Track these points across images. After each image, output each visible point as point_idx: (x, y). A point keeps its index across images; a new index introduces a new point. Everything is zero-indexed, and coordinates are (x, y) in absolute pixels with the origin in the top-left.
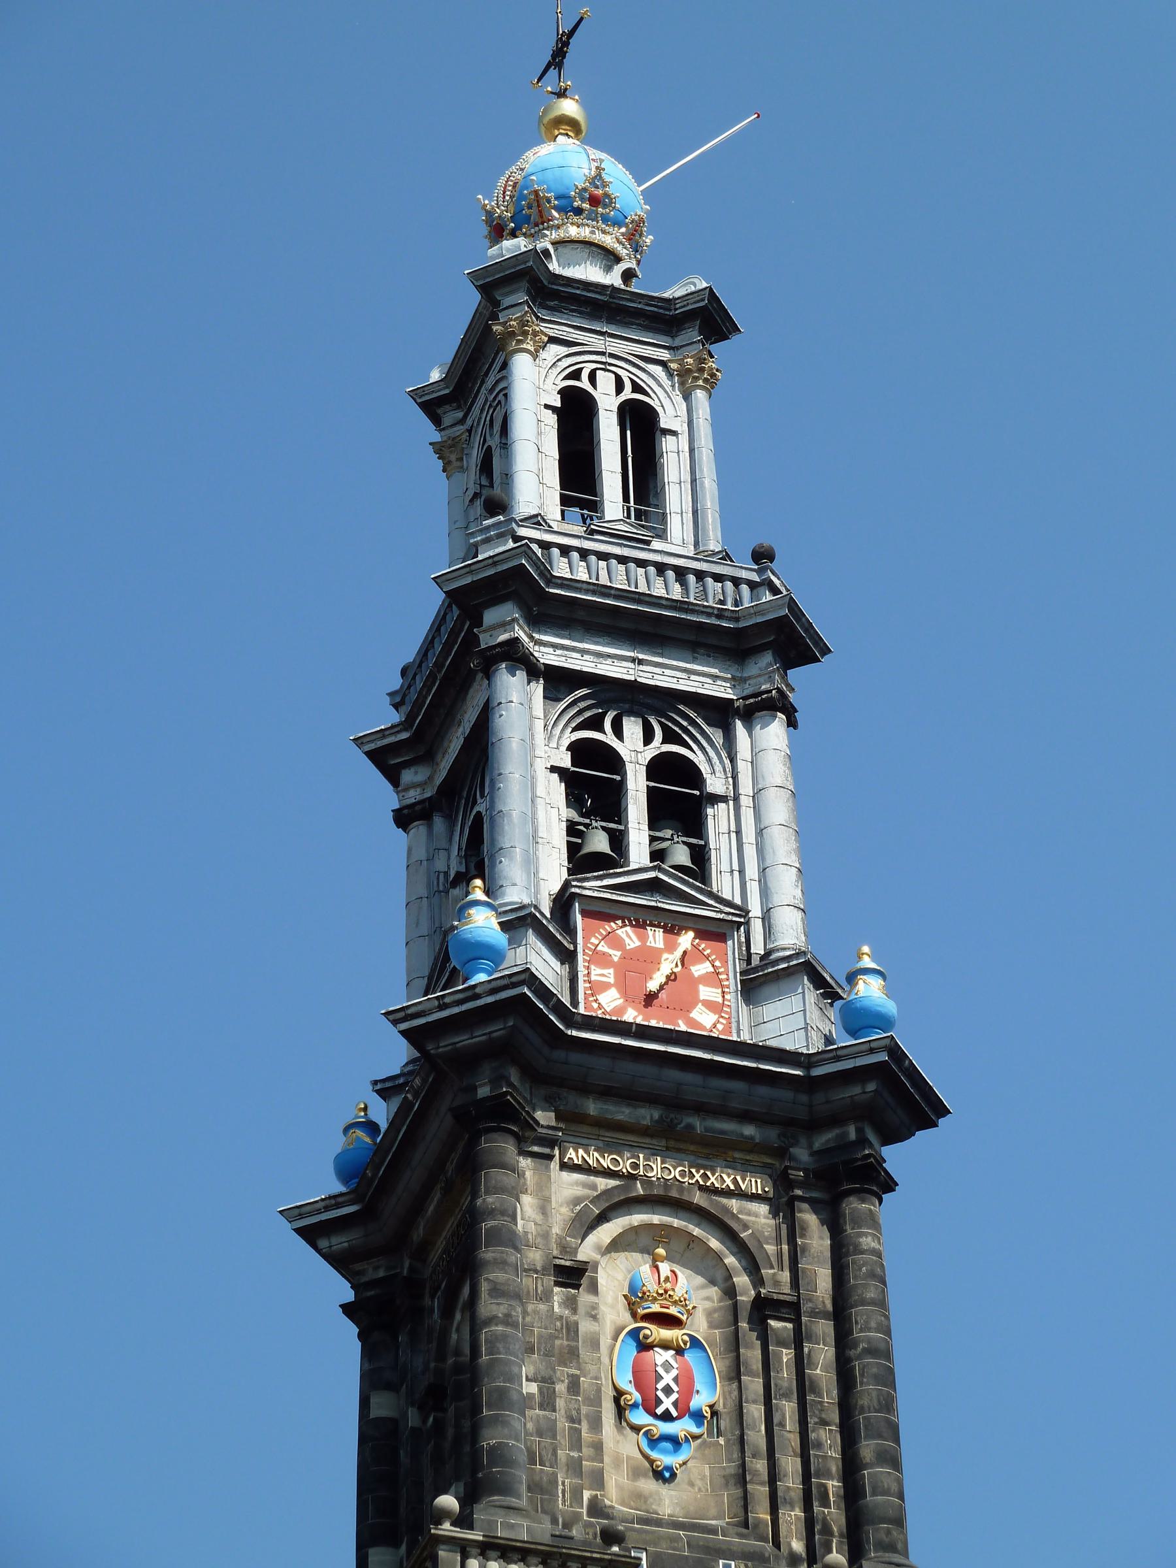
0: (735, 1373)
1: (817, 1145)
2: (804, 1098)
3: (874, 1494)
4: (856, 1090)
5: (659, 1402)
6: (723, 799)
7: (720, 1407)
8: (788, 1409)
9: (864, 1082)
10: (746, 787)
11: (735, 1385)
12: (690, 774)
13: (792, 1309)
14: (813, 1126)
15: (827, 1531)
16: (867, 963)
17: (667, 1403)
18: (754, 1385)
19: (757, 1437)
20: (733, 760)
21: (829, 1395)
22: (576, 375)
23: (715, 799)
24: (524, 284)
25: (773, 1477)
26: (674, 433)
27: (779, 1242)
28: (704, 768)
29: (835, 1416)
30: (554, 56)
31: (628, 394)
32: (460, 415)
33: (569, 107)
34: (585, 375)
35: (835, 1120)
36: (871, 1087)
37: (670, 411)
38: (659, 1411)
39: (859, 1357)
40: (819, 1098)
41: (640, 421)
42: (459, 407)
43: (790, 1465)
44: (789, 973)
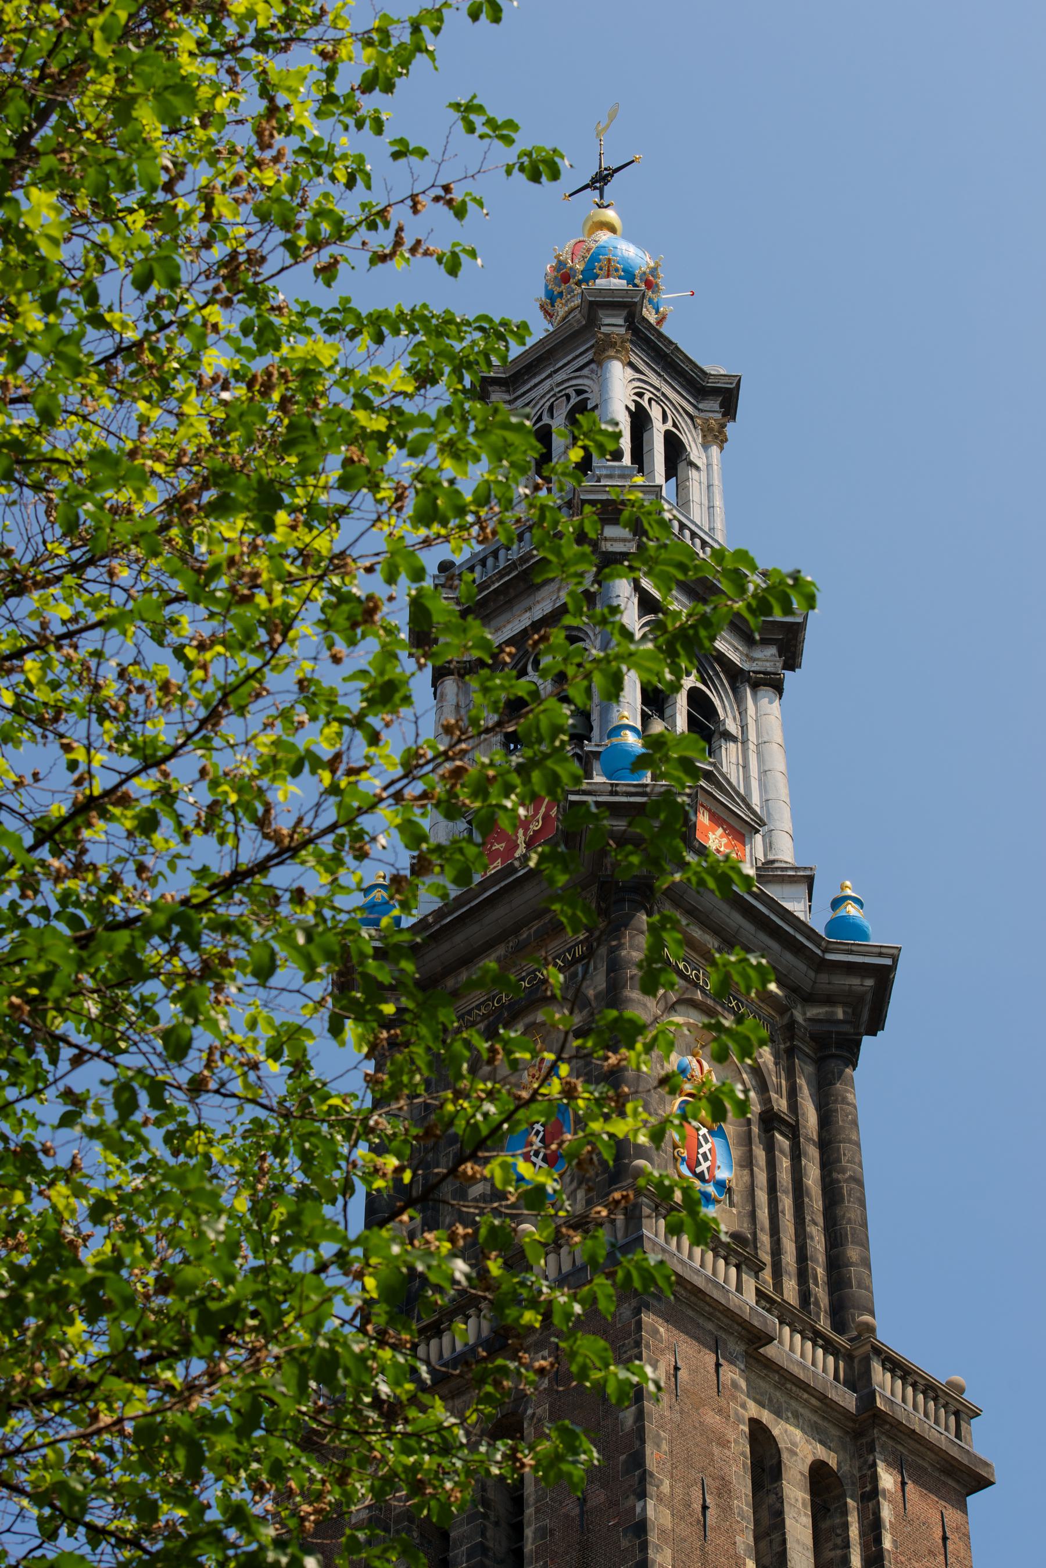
0: (748, 1162)
1: (809, 1015)
2: (812, 974)
3: (859, 1286)
4: (855, 981)
5: (699, 1164)
6: (733, 738)
7: (733, 1185)
8: (786, 1202)
9: (863, 977)
10: (752, 736)
11: (746, 1172)
12: (710, 711)
13: (794, 1132)
14: (809, 999)
15: (817, 1304)
16: (849, 892)
17: (704, 1166)
18: (762, 1177)
19: (763, 1214)
20: (743, 713)
21: (816, 1202)
22: (640, 395)
23: (728, 736)
24: (625, 313)
25: (777, 1251)
26: (697, 468)
27: (778, 1076)
28: (720, 710)
29: (820, 1220)
30: (594, 180)
31: (669, 425)
32: (508, 398)
33: (610, 215)
34: (646, 397)
35: (829, 1000)
36: (869, 982)
37: (695, 452)
38: (698, 1170)
39: (846, 1181)
40: (823, 978)
41: (674, 448)
42: (508, 392)
43: (789, 1246)
44: (793, 880)
